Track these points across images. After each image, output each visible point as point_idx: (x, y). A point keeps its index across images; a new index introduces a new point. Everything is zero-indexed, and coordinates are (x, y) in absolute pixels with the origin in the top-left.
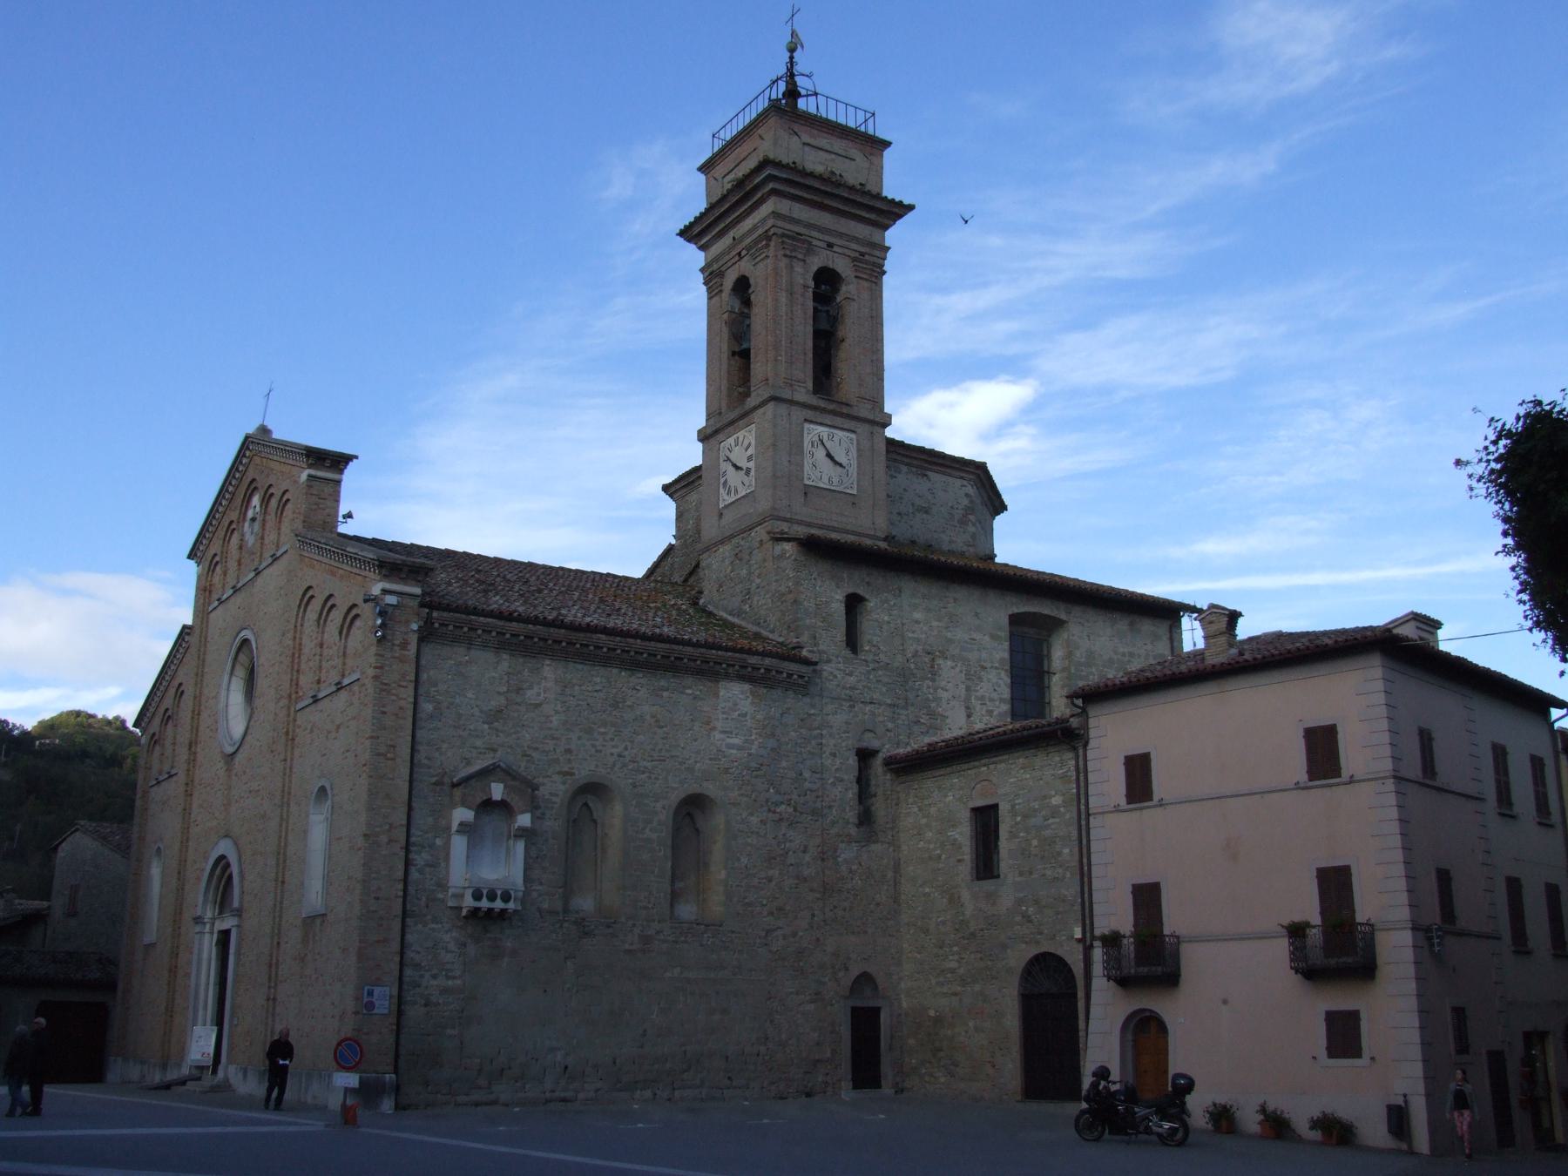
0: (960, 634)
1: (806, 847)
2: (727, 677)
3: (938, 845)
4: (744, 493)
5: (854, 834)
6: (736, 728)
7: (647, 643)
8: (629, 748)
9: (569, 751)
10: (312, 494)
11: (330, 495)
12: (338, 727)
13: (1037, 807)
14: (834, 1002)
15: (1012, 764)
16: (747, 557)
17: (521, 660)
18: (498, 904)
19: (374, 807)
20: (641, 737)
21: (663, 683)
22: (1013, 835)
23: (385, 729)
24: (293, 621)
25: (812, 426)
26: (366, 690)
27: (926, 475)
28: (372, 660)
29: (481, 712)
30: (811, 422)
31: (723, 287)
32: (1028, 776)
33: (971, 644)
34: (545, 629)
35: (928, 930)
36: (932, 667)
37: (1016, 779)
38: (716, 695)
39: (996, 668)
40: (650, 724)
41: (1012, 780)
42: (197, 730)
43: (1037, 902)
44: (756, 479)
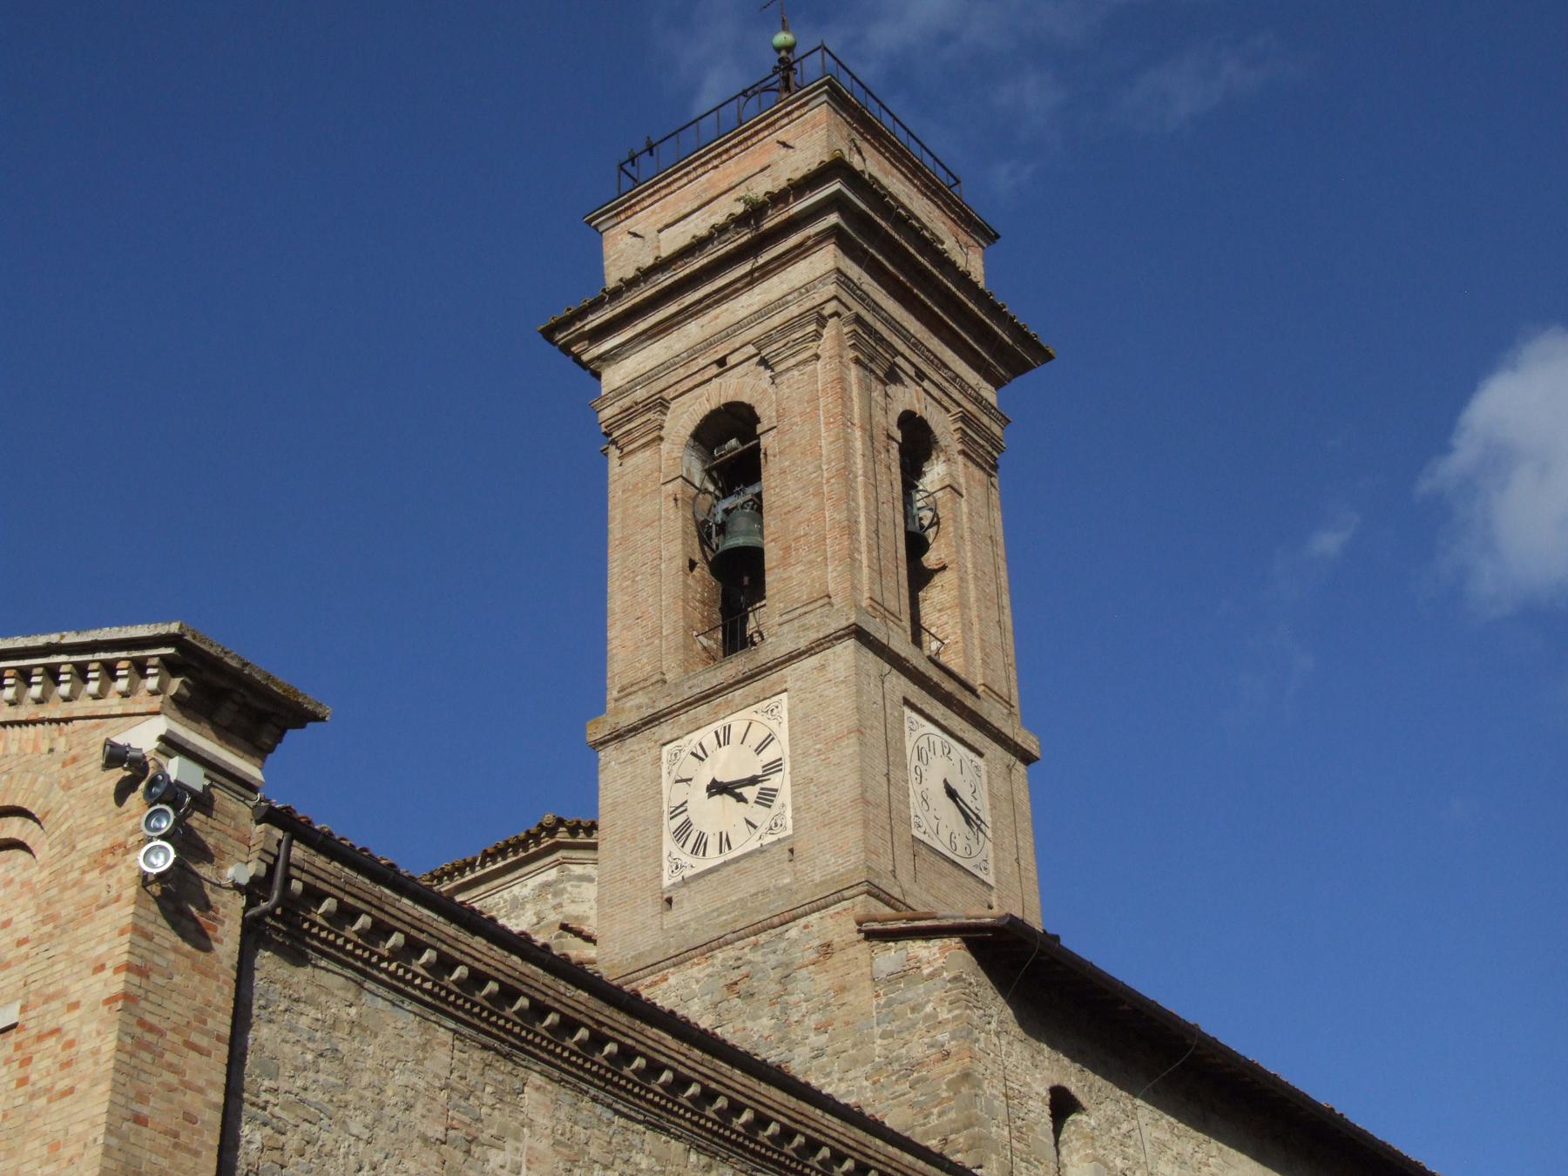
4: (753, 845)
16: (774, 988)
17: (478, 1055)
25: (915, 716)
26: (70, 1044)
28: (119, 949)
30: (914, 707)
31: (663, 433)
34: (549, 979)
44: (796, 810)
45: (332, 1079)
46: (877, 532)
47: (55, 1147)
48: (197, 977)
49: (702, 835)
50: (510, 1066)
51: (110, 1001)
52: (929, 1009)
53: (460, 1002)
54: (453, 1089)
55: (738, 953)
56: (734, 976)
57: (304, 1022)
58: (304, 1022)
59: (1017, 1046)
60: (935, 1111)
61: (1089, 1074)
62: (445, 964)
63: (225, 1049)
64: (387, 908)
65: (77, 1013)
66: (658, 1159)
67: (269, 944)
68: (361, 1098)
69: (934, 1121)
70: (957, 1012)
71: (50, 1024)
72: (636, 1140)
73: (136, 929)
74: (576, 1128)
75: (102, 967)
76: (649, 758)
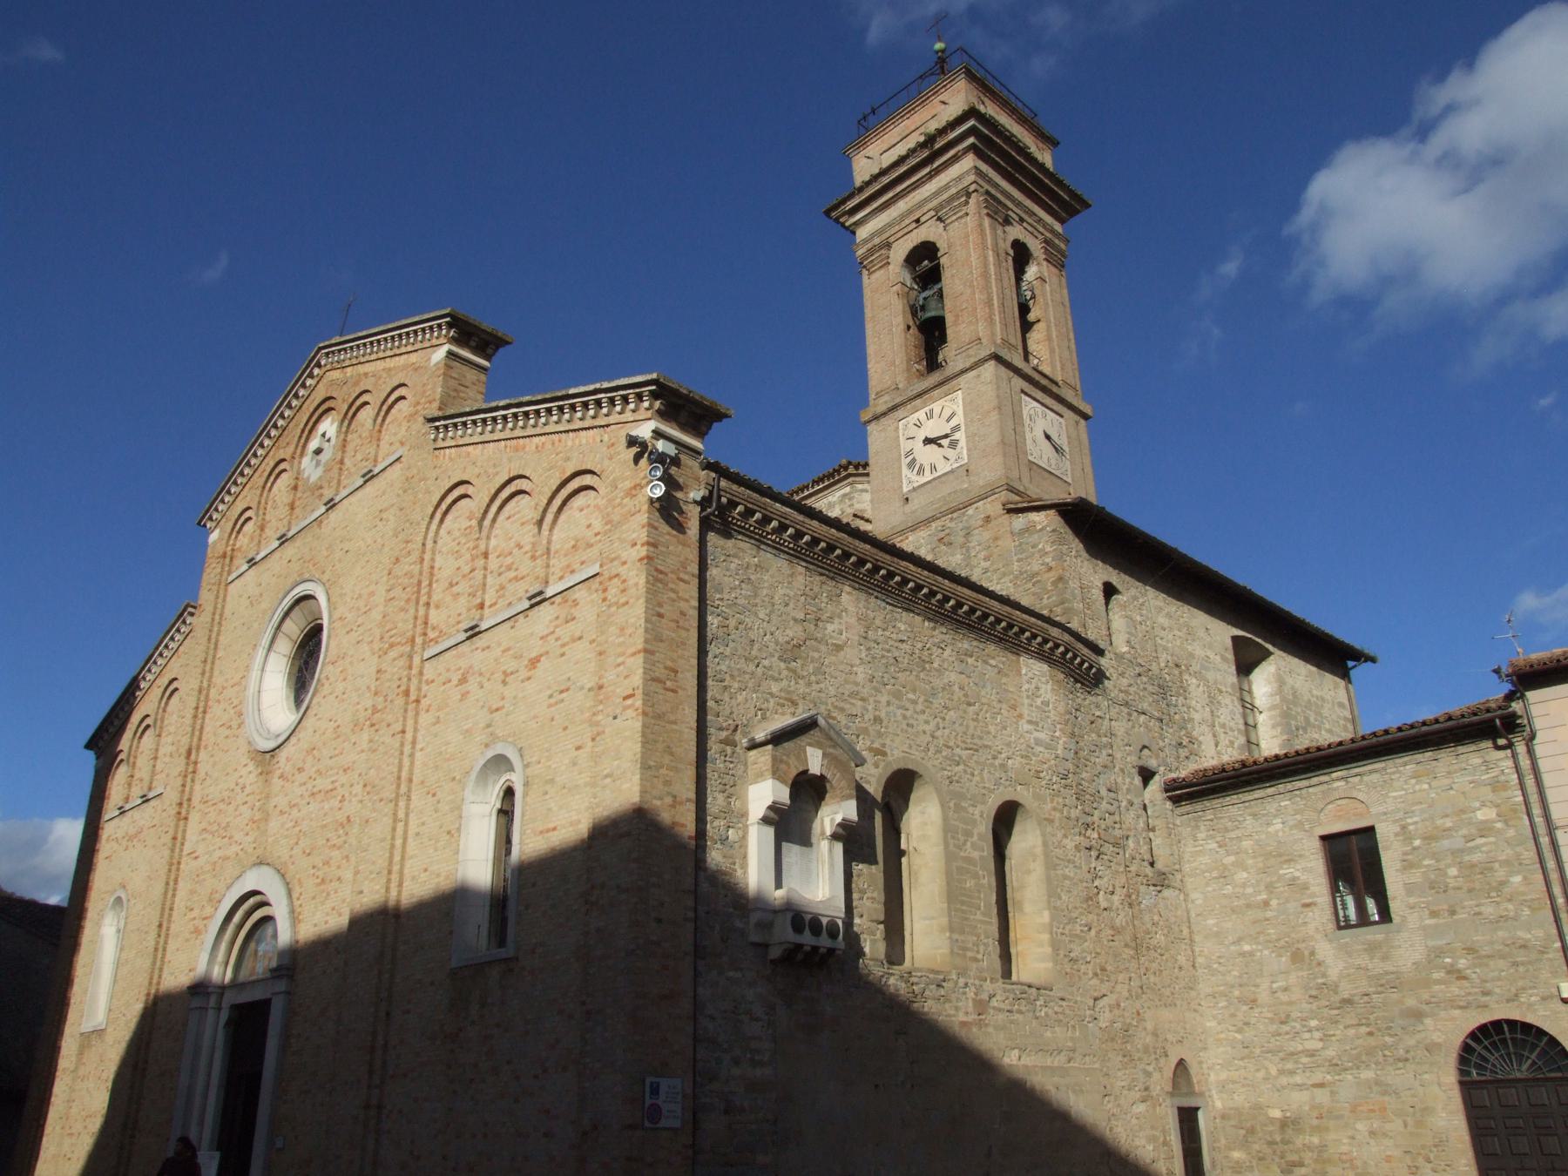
4: (948, 469)
8: (941, 726)
9: (878, 720)
10: (451, 377)
12: (534, 662)
13: (1449, 824)
15: (1394, 773)
16: (962, 540)
17: (818, 578)
19: (652, 763)
22: (1408, 866)
23: (662, 641)
24: (419, 539)
25: (1027, 398)
28: (643, 535)
29: (777, 643)
30: (1026, 394)
32: (1426, 786)
34: (850, 540)
35: (1254, 1001)
36: (1182, 682)
38: (1019, 673)
42: (201, 733)
43: (1470, 950)
44: (969, 450)
46: (1003, 304)
47: (622, 629)
48: (680, 547)
50: (834, 583)
51: (641, 560)
52: (1040, 547)
56: (942, 535)
57: (733, 566)
58: (733, 566)
59: (1086, 563)
61: (1122, 575)
62: (799, 535)
65: (626, 567)
66: (909, 625)
67: (713, 529)
68: (763, 601)
69: (1045, 601)
71: (614, 572)
72: (898, 616)
73: (650, 525)
75: (636, 544)
76: (893, 428)
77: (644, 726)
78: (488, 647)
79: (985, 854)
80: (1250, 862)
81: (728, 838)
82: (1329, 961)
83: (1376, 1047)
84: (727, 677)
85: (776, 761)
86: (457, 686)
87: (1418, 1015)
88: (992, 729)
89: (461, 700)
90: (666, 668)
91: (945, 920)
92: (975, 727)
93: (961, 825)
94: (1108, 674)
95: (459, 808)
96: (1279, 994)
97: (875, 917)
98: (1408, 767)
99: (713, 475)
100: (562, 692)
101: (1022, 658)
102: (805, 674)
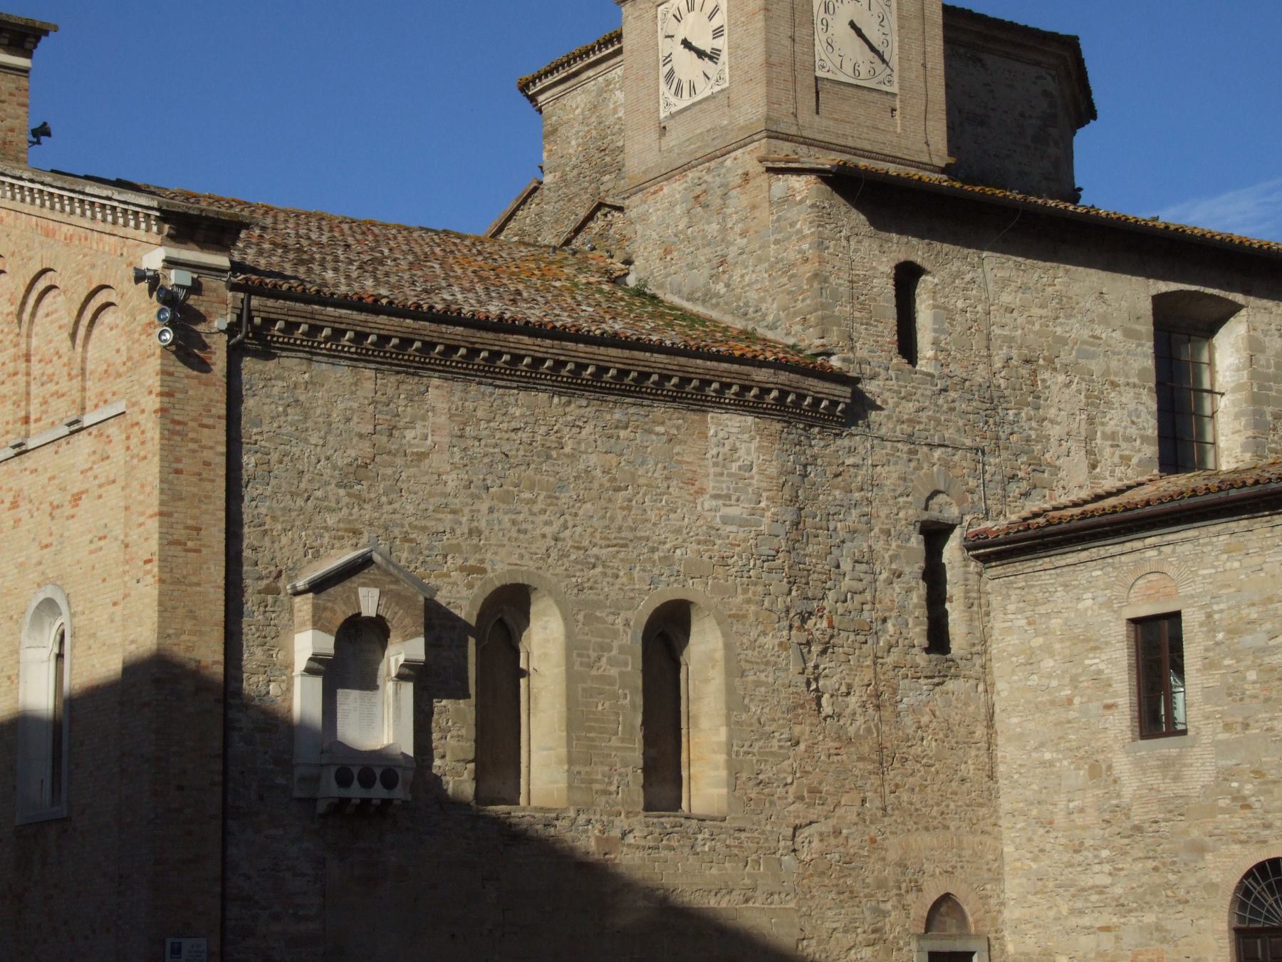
0: (1076, 330)
1: (849, 686)
2: (718, 403)
3: (1067, 680)
4: (707, 93)
5: (923, 664)
6: (736, 490)
7: (594, 349)
8: (570, 524)
9: (474, 532)
11: (11, 94)
12: (77, 498)
13: (1254, 616)
14: (901, 943)
15: (1205, 545)
16: (719, 201)
17: (393, 379)
18: (378, 792)
19: (171, 631)
20: (588, 505)
21: (618, 414)
22: (1209, 665)
23: (181, 499)
26: (143, 432)
27: (980, 60)
28: (155, 382)
29: (334, 467)
32: (1236, 564)
33: (1092, 345)
34: (434, 326)
35: (1051, 823)
37: (1213, 571)
38: (704, 435)
39: (1135, 386)
40: (601, 485)
41: (1205, 572)
43: (1258, 773)
44: (730, 68)
45: (296, 418)
48: (203, 388)
49: (680, 81)
50: (416, 379)
51: (155, 412)
52: (798, 226)
53: (376, 353)
54: (377, 403)
55: (698, 174)
56: (698, 190)
57: (276, 390)
58: (276, 390)
60: (800, 298)
61: (937, 245)
62: (360, 337)
63: (224, 422)
64: (317, 317)
66: (528, 408)
67: (249, 353)
69: (799, 305)
70: (813, 230)
71: (135, 420)
72: (512, 400)
73: (164, 373)
74: (467, 404)
75: (150, 392)
76: (649, 15)
77: (161, 594)
78: (36, 470)
79: (629, 668)
80: (1057, 646)
81: (268, 693)
82: (1125, 778)
83: (1159, 885)
84: (268, 519)
85: (316, 609)
86: (9, 509)
87: (1199, 849)
88: (652, 516)
89: (14, 527)
90: (187, 528)
91: (563, 751)
92: (625, 518)
93: (594, 640)
94: (879, 402)
95: (17, 652)
96: (1075, 816)
97: (462, 756)
98: (1221, 538)
99: (241, 295)
100: (100, 539)
101: (710, 415)
102: (373, 496)
